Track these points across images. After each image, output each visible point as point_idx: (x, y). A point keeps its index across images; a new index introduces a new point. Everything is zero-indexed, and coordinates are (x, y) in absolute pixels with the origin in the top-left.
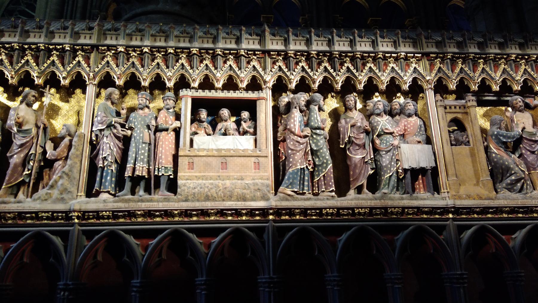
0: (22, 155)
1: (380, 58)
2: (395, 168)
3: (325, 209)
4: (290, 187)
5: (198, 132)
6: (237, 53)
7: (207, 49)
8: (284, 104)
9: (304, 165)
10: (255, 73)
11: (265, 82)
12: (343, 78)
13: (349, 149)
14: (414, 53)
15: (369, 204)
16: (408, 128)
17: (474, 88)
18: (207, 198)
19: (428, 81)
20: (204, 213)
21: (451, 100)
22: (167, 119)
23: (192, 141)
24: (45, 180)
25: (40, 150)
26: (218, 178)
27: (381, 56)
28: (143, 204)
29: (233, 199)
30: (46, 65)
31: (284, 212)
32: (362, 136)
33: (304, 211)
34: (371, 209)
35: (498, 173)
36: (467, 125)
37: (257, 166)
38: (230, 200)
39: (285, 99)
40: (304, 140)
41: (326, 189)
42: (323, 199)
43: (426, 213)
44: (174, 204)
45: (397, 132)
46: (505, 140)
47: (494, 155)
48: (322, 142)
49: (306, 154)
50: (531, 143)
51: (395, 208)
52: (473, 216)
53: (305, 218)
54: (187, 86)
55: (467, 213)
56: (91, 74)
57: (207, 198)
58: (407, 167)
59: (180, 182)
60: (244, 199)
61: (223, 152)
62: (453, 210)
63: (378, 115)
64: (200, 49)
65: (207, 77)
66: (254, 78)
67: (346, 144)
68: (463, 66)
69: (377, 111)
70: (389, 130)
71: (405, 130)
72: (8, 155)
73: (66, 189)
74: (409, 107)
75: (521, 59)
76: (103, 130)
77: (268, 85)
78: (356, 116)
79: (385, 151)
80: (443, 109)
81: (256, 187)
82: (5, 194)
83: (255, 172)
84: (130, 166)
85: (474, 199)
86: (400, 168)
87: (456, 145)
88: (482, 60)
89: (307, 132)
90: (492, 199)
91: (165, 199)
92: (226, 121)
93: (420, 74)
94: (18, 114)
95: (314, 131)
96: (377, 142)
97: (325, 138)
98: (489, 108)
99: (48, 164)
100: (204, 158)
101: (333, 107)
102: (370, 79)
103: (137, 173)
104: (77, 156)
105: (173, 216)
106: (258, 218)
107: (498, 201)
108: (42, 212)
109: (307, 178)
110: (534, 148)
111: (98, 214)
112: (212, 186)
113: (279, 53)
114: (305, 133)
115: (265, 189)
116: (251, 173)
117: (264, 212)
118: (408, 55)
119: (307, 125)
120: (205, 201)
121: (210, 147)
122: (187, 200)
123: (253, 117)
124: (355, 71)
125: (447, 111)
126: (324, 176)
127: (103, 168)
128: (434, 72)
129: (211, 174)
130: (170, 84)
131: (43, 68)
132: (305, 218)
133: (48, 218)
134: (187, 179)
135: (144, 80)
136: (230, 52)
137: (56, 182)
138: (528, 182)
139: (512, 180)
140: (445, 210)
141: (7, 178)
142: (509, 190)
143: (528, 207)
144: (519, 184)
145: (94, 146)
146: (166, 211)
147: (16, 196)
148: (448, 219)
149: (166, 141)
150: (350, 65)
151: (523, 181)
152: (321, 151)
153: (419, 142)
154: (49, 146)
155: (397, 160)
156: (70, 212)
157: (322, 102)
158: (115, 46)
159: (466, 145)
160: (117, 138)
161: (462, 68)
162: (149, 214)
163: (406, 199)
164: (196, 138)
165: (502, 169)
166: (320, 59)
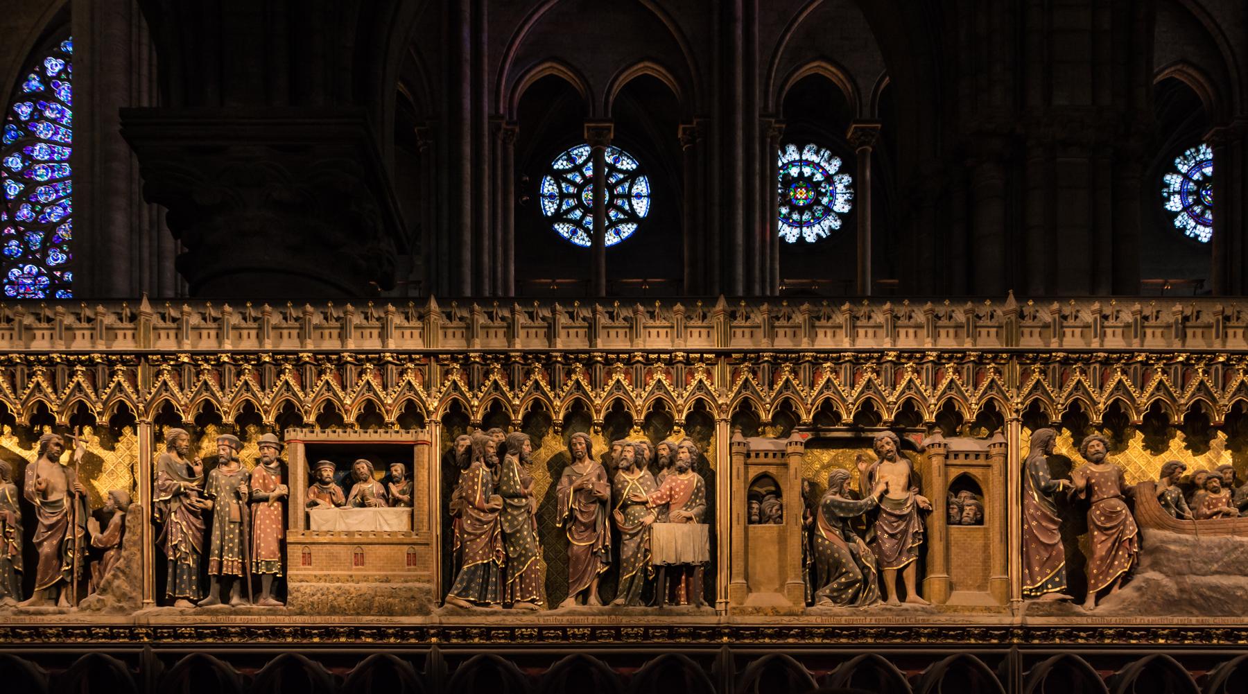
0: (55, 542)
1: (638, 362)
5: (319, 501)
6: (380, 359)
7: (327, 353)
8: (462, 450)
10: (410, 395)
11: (429, 413)
12: (569, 401)
14: (702, 352)
16: (676, 493)
17: (806, 418)
18: (333, 611)
19: (720, 406)
20: (328, 632)
22: (267, 482)
23: (307, 517)
24: (95, 580)
25: (80, 534)
28: (238, 617)
30: (67, 391)
33: (486, 632)
34: (594, 629)
35: (818, 571)
37: (412, 559)
38: (369, 615)
39: (464, 441)
40: (490, 516)
41: (522, 597)
42: (517, 613)
43: (685, 635)
44: (286, 620)
45: (654, 502)
49: (493, 539)
50: (893, 519)
51: (633, 628)
54: (298, 422)
55: (755, 636)
56: (141, 406)
57: (333, 611)
59: (291, 585)
60: (391, 613)
61: (357, 536)
64: (315, 353)
65: (329, 405)
67: (565, 522)
69: (624, 464)
71: (671, 496)
72: (35, 540)
73: (124, 594)
75: (909, 359)
76: (169, 501)
77: (433, 417)
78: (589, 470)
81: (410, 594)
82: (41, 599)
84: (214, 559)
87: (760, 522)
89: (497, 502)
93: (708, 393)
94: (38, 477)
96: (619, 517)
97: (529, 513)
99: (95, 554)
100: (328, 547)
102: (618, 403)
103: (224, 571)
104: (135, 543)
105: (284, 636)
106: (413, 641)
111: (175, 631)
113: (454, 356)
114: (492, 505)
115: (423, 597)
117: (422, 632)
118: (692, 356)
119: (496, 490)
121: (338, 529)
122: (302, 613)
123: (410, 475)
124: (588, 389)
125: (749, 461)
127: (175, 562)
128: (735, 389)
129: (339, 572)
130: (269, 419)
131: (64, 397)
133: (105, 636)
135: (225, 413)
137: (109, 583)
139: (840, 584)
141: (39, 577)
143: (857, 629)
145: (160, 527)
146: (272, 628)
147: (57, 602)
148: (720, 646)
149: (267, 516)
150: (581, 378)
153: (689, 519)
154: (93, 525)
156: (136, 627)
157: (527, 448)
158: (173, 353)
160: (193, 513)
162: (248, 631)
164: (314, 512)
165: (828, 563)
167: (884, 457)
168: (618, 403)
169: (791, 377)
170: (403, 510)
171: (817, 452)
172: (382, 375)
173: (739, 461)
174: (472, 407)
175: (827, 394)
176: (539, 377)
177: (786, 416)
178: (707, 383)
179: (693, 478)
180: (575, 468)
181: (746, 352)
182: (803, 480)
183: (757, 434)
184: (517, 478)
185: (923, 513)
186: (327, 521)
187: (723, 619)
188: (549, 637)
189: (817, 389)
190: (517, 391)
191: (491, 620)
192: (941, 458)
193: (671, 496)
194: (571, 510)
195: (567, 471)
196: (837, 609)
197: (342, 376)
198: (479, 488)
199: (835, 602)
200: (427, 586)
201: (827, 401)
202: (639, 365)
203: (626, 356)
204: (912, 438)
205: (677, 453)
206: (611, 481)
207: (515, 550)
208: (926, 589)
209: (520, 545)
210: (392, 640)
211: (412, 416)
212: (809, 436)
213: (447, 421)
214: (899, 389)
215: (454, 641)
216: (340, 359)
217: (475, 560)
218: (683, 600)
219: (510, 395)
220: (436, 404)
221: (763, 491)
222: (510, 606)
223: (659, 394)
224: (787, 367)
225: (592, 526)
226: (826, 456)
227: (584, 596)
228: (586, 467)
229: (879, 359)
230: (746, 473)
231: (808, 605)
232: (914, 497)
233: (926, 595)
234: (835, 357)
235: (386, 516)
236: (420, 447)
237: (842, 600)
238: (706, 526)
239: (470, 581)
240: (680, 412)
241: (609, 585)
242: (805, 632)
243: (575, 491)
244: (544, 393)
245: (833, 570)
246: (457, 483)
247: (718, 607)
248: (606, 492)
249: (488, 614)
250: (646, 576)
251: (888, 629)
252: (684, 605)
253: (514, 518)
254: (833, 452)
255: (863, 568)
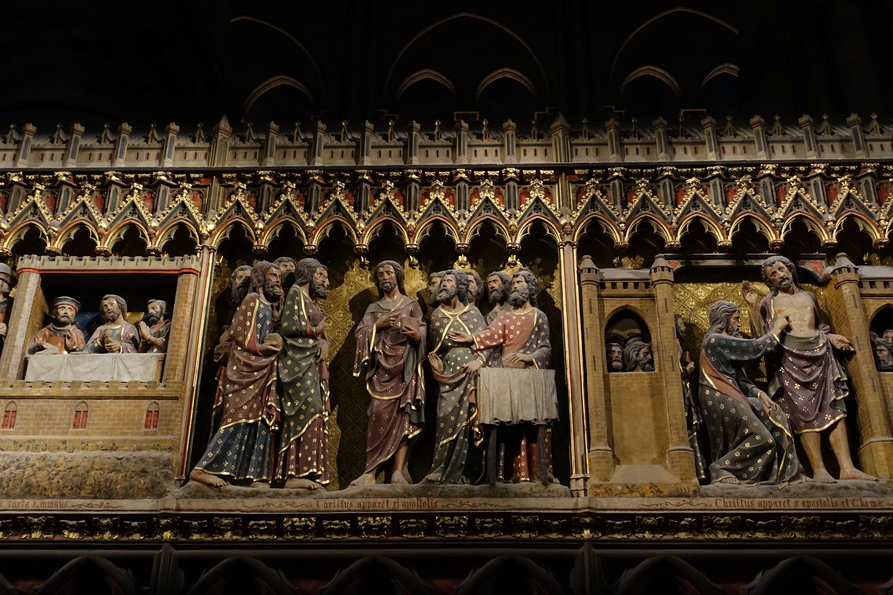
1: (462, 179)
2: (464, 424)
3: (291, 516)
4: (215, 466)
5: (45, 345)
6: (152, 179)
7: (89, 172)
8: (239, 282)
9: (256, 417)
13: (371, 379)
14: (538, 168)
15: (391, 506)
16: (511, 332)
18: (29, 491)
19: (563, 227)
21: (626, 271)
23: (25, 363)
26: (62, 446)
27: (464, 176)
29: (83, 494)
31: (195, 523)
32: (403, 350)
33: (242, 522)
34: (396, 517)
35: (712, 435)
36: (650, 325)
37: (153, 419)
38: (78, 497)
40: (264, 361)
42: (288, 495)
43: (528, 527)
45: (481, 342)
46: (733, 358)
47: (707, 392)
48: (304, 364)
49: (264, 391)
50: (804, 363)
51: (452, 515)
52: (640, 536)
53: (244, 539)
57: (29, 491)
58: (487, 422)
61: (84, 388)
62: (588, 520)
63: (448, 303)
64: (74, 172)
66: (182, 229)
67: (364, 369)
68: (649, 194)
69: (444, 295)
70: (463, 337)
71: (504, 336)
74: (516, 285)
75: (791, 173)
77: (207, 243)
78: (398, 306)
79: (449, 385)
80: (595, 288)
83: (146, 434)
85: (643, 496)
86: (477, 423)
88: (693, 179)
89: (275, 341)
90: (689, 496)
92: (113, 321)
93: (548, 213)
95: (289, 341)
96: (436, 363)
97: (317, 357)
98: (720, 285)
100: (41, 402)
101: (362, 289)
102: (437, 226)
106: (137, 537)
107: (702, 500)
109: (262, 447)
110: (810, 375)
112: (43, 464)
113: (240, 174)
114: (267, 345)
116: (136, 434)
117: (149, 523)
118: (525, 172)
119: (276, 327)
120: (22, 496)
121: (63, 378)
123: (168, 315)
125: (604, 293)
126: (298, 440)
128: (581, 207)
132: (244, 539)
136: (136, 177)
138: (790, 456)
139: (744, 452)
140: (571, 521)
142: (738, 474)
143: (777, 516)
144: (759, 461)
148: (581, 542)
151: (769, 452)
152: (298, 385)
153: (529, 364)
155: (471, 405)
159: (644, 370)
161: (644, 197)
163: (479, 495)
166: (331, 185)
167: (777, 288)
168: (437, 226)
169: (649, 194)
170: (154, 355)
171: (690, 287)
172: (153, 198)
173: (590, 291)
174: (255, 230)
175: (694, 213)
176: (340, 197)
177: (646, 244)
178: (546, 201)
179: (532, 314)
180: (381, 304)
181: (591, 167)
182: (677, 317)
183: (612, 266)
184: (304, 312)
185: (844, 356)
186: (49, 369)
187: (582, 502)
188: (331, 531)
189: (682, 206)
190: (313, 213)
191: (250, 505)
192: (854, 286)
193: (504, 336)
194: (373, 354)
195: (372, 308)
196: (744, 487)
197: (104, 199)
198: (252, 324)
199: (740, 478)
200: (167, 455)
201: (696, 221)
202: (463, 184)
203: (447, 173)
204: (809, 266)
205: (512, 283)
206: (428, 321)
207: (293, 404)
208: (866, 459)
209: (299, 398)
210: (107, 536)
211: (182, 242)
212: (678, 265)
213: (224, 249)
214: (785, 205)
215: (196, 537)
216: (103, 180)
217: (234, 417)
218: (523, 476)
219: (304, 217)
220: (211, 226)
221: (624, 334)
222: (281, 484)
223: (485, 215)
224: (642, 183)
225: (398, 374)
226: (703, 291)
227: (386, 471)
228: (395, 302)
229: (754, 174)
230: (601, 307)
231: (703, 482)
232: (823, 336)
233: (868, 468)
234: (702, 172)
235: (129, 363)
236: (184, 276)
237: (750, 474)
238: (552, 373)
239: (226, 447)
240: (513, 234)
241: (420, 455)
242: (702, 522)
243: (378, 331)
244: (346, 215)
245: (731, 432)
246: (230, 323)
247: (573, 484)
248: (421, 332)
249: (246, 496)
250: (472, 441)
251: (824, 516)
252: (524, 482)
253: (296, 363)
254: (710, 287)
255: (774, 429)
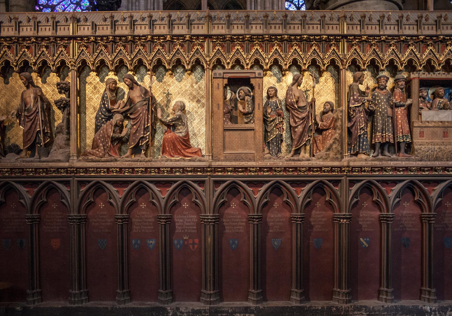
18: (437, 159)
20: (432, 169)
61: (446, 123)
91: (406, 159)
100: (432, 128)
108: (325, 167)
120: (434, 161)
122: (421, 161)
129: (437, 141)
133: (328, 171)
134: (420, 145)
162: (395, 169)
